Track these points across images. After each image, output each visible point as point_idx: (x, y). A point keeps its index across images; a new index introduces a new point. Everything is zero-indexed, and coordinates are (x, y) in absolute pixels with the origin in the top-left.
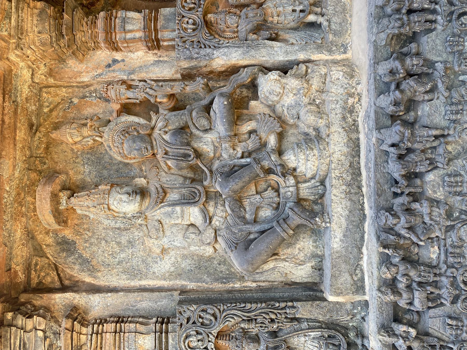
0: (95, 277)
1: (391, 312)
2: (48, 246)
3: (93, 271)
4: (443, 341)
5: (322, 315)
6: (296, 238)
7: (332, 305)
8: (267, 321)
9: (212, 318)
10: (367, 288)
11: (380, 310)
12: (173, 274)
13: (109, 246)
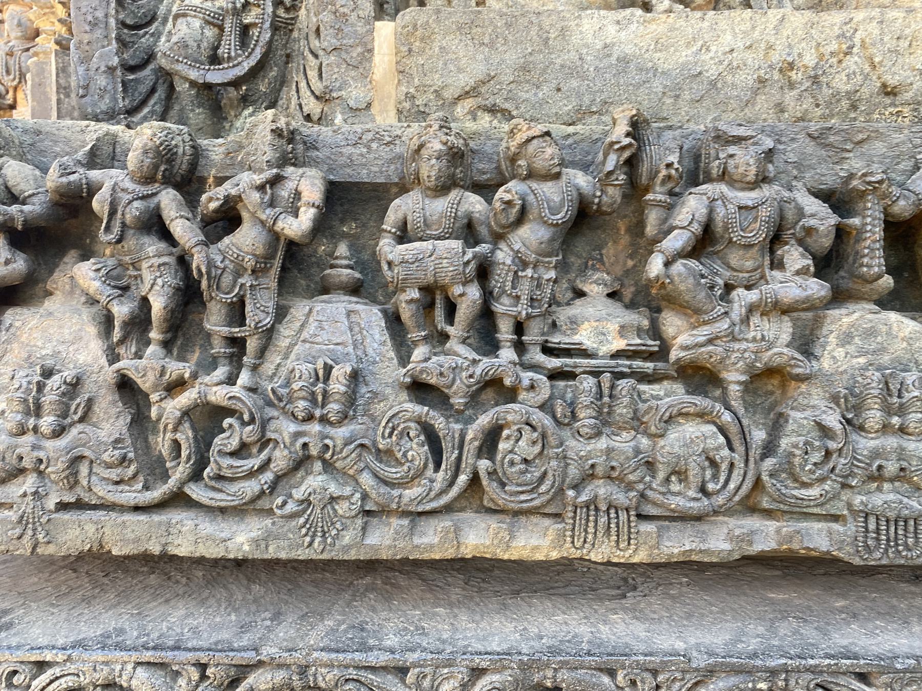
1: (364, 176)
4: (262, 353)
7: (361, 29)
11: (370, 136)
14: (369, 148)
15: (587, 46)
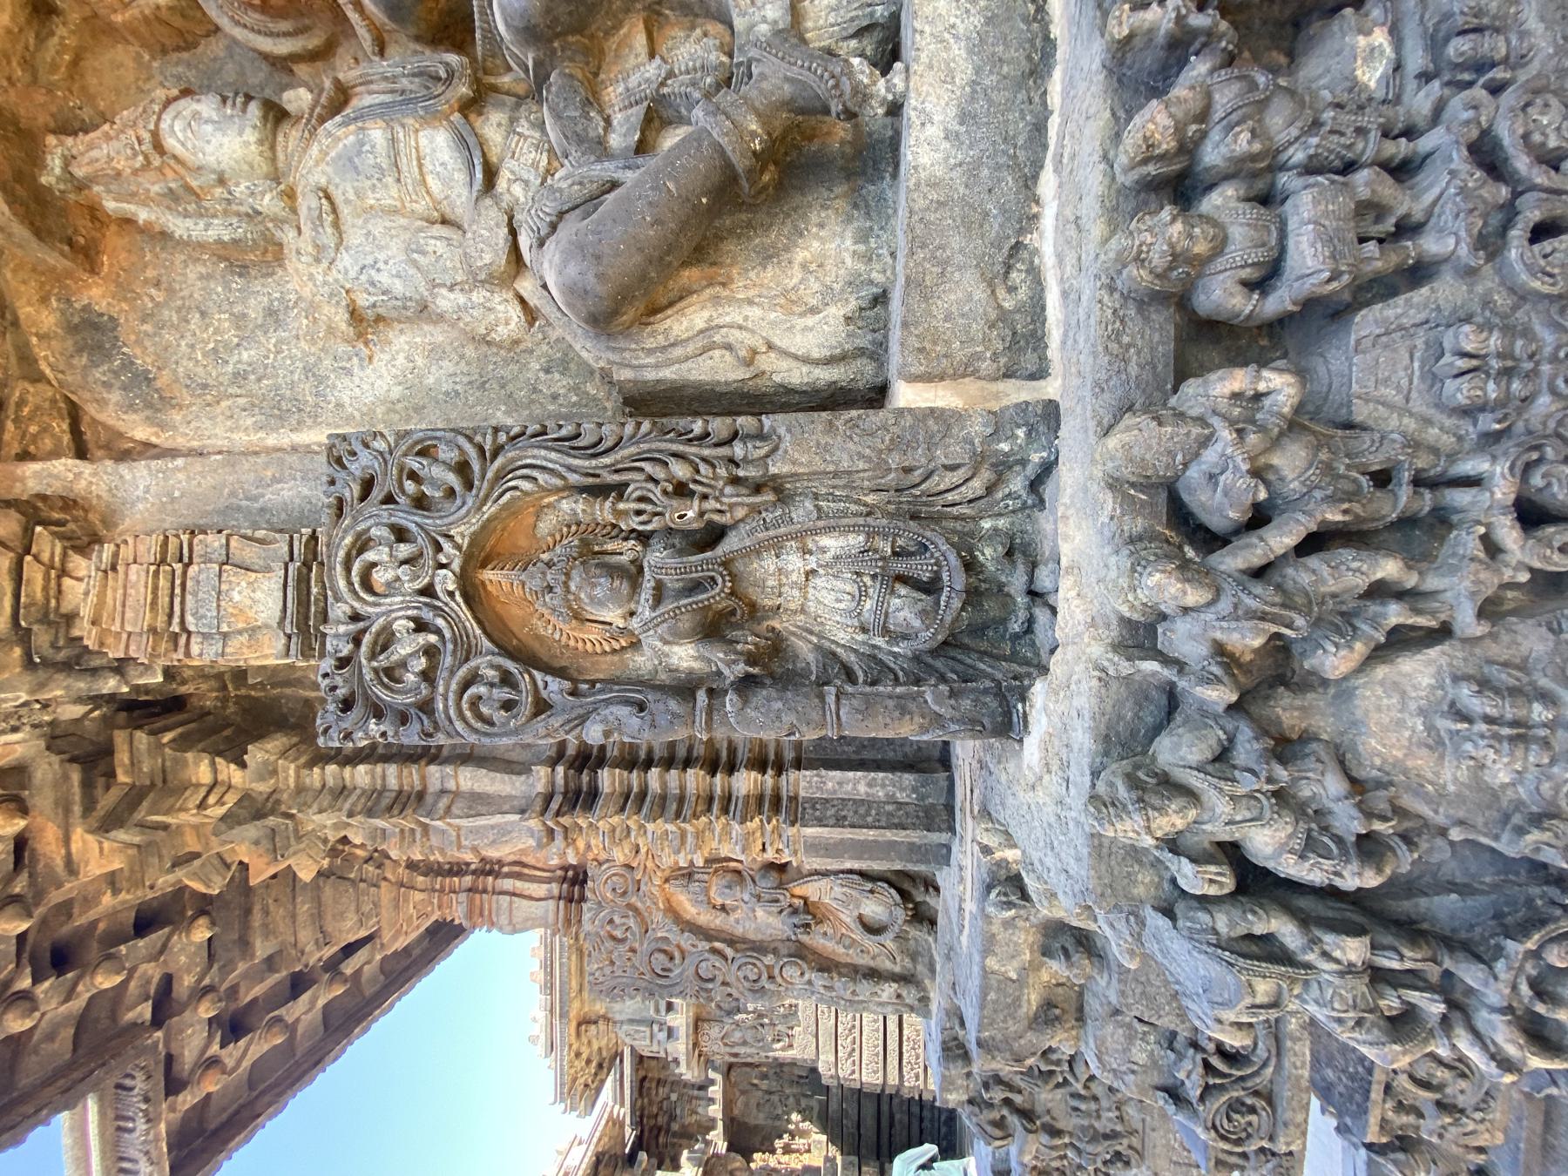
0: (163, 426)
2: (40, 337)
3: (157, 403)
5: (869, 459)
6: (795, 227)
7: (908, 421)
8: (658, 491)
9: (452, 479)
10: (1054, 352)
11: (1114, 347)
12: (399, 406)
13: (207, 326)
14: (1129, 346)
15: (946, 159)
